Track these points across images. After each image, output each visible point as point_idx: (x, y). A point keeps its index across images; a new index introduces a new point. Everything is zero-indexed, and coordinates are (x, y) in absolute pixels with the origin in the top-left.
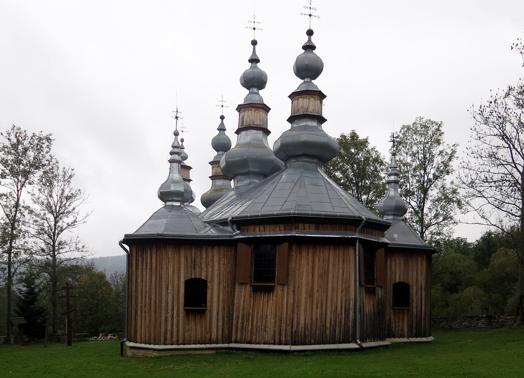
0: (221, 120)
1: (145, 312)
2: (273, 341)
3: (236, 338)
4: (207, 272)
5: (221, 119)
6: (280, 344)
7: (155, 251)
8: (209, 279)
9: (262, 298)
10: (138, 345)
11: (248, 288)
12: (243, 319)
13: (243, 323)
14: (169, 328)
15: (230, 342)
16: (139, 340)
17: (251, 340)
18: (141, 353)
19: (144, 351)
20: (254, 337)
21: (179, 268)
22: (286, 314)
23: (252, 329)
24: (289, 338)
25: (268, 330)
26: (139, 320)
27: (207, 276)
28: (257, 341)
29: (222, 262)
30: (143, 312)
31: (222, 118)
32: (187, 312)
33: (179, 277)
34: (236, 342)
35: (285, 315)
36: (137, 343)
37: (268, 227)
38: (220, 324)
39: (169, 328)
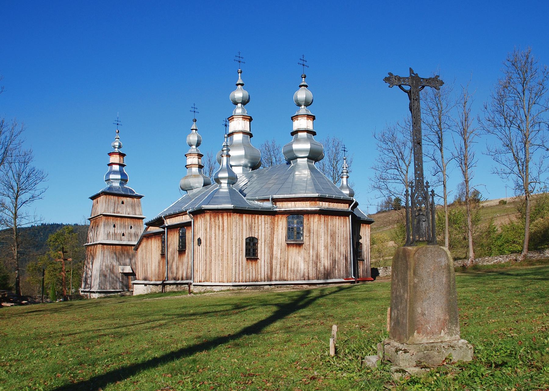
3: (276, 278)
4: (258, 233)
7: (226, 218)
8: (260, 238)
14: (237, 271)
15: (271, 280)
17: (288, 278)
20: (289, 276)
21: (242, 229)
26: (213, 266)
27: (258, 235)
28: (292, 279)
29: (266, 227)
30: (217, 260)
32: (247, 259)
33: (242, 236)
34: (276, 280)
38: (266, 268)
39: (237, 271)
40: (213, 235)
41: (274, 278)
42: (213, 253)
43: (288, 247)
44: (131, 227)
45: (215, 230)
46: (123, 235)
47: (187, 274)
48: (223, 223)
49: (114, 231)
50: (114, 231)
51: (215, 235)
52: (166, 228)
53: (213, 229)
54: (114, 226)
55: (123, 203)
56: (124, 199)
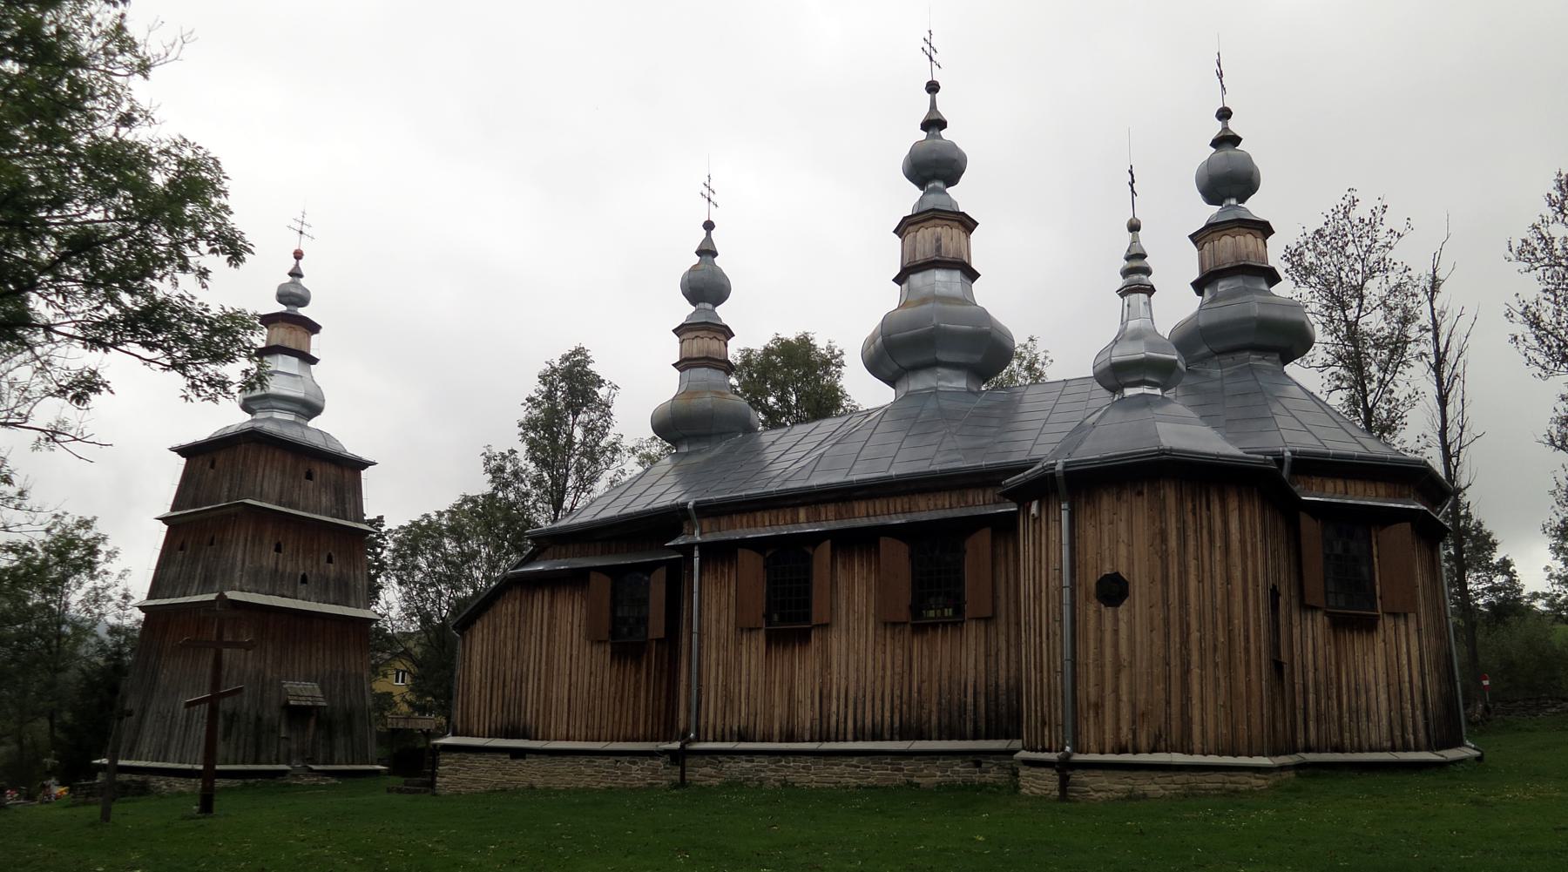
0: (705, 232)
1: (1216, 665)
2: (1389, 744)
3: (1307, 738)
5: (705, 229)
6: (1406, 748)
9: (1357, 645)
10: (1197, 759)
11: (1321, 620)
12: (1317, 692)
13: (1318, 703)
16: (1197, 743)
18: (1212, 781)
19: (1219, 777)
22: (1411, 682)
23: (1340, 717)
24: (1422, 734)
25: (1374, 718)
31: (709, 226)
34: (1308, 749)
35: (1407, 685)
36: (1191, 752)
37: (1353, 486)
40: (1192, 564)
41: (1300, 741)
42: (1195, 635)
43: (1335, 632)
44: (330, 560)
45: (1199, 546)
46: (304, 580)
47: (823, 715)
48: (1226, 523)
49: (277, 564)
50: (277, 564)
51: (1200, 568)
52: (696, 553)
53: (1191, 543)
54: (278, 549)
55: (309, 476)
56: (317, 469)
